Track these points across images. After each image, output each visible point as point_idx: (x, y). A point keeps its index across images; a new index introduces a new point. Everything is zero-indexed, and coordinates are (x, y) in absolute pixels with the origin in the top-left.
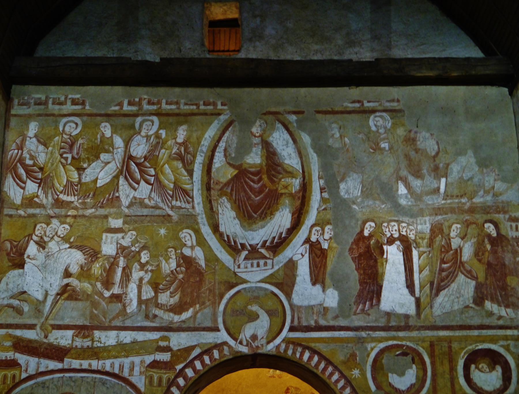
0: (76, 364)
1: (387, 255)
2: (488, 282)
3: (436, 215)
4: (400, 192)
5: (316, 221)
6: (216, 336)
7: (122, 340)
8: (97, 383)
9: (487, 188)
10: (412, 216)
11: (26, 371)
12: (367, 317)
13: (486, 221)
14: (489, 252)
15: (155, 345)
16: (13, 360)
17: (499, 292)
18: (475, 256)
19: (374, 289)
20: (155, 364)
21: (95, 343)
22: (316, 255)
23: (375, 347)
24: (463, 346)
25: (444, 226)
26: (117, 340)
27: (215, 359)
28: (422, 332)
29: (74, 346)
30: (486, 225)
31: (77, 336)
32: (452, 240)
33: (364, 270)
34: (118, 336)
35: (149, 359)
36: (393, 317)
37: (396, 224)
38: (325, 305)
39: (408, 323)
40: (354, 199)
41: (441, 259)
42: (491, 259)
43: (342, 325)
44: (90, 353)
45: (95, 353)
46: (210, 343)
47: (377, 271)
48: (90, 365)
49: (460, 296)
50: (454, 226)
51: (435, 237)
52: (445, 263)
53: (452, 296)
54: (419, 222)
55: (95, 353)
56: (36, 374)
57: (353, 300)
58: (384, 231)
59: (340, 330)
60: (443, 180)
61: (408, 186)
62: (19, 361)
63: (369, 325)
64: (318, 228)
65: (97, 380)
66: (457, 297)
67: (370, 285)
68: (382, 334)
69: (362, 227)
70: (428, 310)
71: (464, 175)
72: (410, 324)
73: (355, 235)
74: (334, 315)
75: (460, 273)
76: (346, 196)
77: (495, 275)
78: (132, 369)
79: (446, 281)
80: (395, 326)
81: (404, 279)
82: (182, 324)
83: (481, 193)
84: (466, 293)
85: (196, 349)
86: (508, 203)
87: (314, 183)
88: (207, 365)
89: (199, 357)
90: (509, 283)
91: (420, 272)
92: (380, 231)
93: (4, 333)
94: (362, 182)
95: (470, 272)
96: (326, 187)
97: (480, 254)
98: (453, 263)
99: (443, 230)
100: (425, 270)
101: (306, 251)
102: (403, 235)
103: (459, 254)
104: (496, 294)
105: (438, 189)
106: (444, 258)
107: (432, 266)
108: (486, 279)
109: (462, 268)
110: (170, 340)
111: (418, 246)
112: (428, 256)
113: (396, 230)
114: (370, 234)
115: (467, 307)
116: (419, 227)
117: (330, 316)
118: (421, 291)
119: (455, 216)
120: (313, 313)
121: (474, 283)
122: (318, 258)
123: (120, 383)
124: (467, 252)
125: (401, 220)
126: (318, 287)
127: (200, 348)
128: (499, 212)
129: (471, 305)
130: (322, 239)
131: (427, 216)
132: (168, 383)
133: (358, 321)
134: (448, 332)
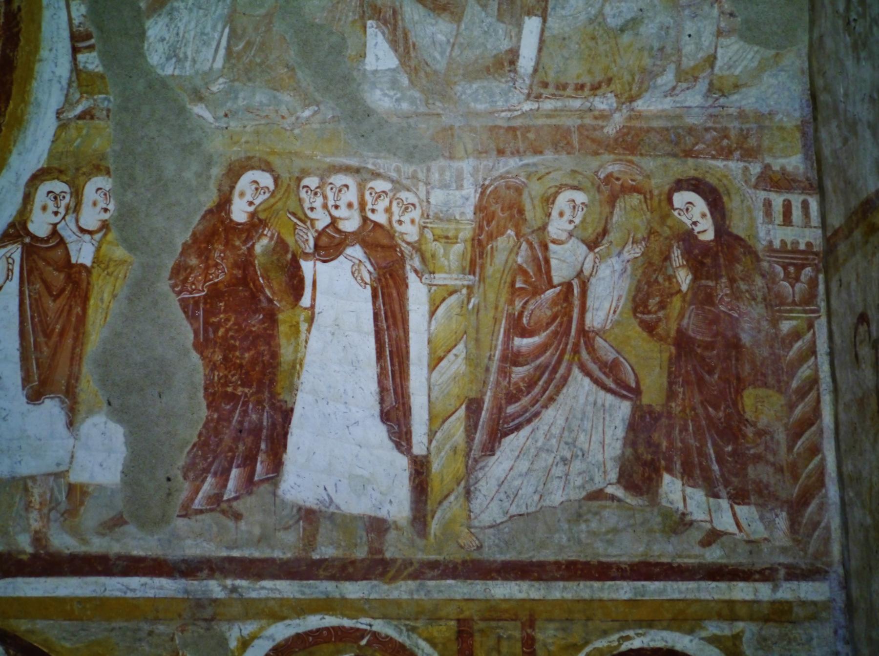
1: (314, 299)
2: (676, 407)
3: (501, 152)
4: (370, 63)
5: (51, 155)
9: (688, 63)
10: (410, 157)
12: (231, 524)
13: (680, 185)
17: (715, 444)
18: (635, 311)
19: (260, 420)
22: (48, 287)
23: (254, 637)
24: (576, 639)
28: (431, 583)
30: (680, 199)
32: (552, 246)
36: (325, 528)
37: (349, 180)
38: (77, 477)
39: (380, 551)
40: (198, 82)
41: (510, 316)
42: (691, 323)
43: (135, 553)
47: (274, 355)
49: (574, 456)
50: (563, 200)
51: (491, 237)
52: (525, 333)
57: (182, 460)
58: (306, 205)
59: (125, 573)
60: (532, 25)
61: (401, 42)
63: (236, 554)
64: (58, 186)
66: (564, 460)
67: (245, 404)
68: (286, 588)
69: (226, 188)
70: (453, 506)
71: (607, 9)
72: (388, 555)
73: (198, 218)
74: (107, 514)
75: (576, 371)
76: (169, 71)
77: (701, 382)
79: (525, 400)
80: (334, 560)
81: (374, 387)
83: (668, 78)
86: (760, 117)
87: (47, 14)
90: (749, 415)
92: (292, 204)
94: (230, 19)
95: (612, 368)
96: (92, 29)
97: (653, 302)
98: (555, 333)
99: (521, 212)
100: (451, 356)
101: (10, 271)
102: (377, 225)
103: (577, 302)
104: (702, 453)
105: (513, 56)
106: (521, 314)
107: (477, 340)
108: (671, 395)
111: (428, 266)
112: (463, 305)
113: (350, 205)
114: (253, 215)
115: (597, 495)
116: (438, 197)
117: (91, 516)
118: (431, 435)
119: (567, 162)
120: (28, 507)
121: (625, 408)
122: (56, 298)
124: (607, 296)
125: (370, 166)
126: (52, 409)
128: (727, 154)
129: (610, 490)
131: (467, 155)
133: (194, 541)
134: (525, 585)
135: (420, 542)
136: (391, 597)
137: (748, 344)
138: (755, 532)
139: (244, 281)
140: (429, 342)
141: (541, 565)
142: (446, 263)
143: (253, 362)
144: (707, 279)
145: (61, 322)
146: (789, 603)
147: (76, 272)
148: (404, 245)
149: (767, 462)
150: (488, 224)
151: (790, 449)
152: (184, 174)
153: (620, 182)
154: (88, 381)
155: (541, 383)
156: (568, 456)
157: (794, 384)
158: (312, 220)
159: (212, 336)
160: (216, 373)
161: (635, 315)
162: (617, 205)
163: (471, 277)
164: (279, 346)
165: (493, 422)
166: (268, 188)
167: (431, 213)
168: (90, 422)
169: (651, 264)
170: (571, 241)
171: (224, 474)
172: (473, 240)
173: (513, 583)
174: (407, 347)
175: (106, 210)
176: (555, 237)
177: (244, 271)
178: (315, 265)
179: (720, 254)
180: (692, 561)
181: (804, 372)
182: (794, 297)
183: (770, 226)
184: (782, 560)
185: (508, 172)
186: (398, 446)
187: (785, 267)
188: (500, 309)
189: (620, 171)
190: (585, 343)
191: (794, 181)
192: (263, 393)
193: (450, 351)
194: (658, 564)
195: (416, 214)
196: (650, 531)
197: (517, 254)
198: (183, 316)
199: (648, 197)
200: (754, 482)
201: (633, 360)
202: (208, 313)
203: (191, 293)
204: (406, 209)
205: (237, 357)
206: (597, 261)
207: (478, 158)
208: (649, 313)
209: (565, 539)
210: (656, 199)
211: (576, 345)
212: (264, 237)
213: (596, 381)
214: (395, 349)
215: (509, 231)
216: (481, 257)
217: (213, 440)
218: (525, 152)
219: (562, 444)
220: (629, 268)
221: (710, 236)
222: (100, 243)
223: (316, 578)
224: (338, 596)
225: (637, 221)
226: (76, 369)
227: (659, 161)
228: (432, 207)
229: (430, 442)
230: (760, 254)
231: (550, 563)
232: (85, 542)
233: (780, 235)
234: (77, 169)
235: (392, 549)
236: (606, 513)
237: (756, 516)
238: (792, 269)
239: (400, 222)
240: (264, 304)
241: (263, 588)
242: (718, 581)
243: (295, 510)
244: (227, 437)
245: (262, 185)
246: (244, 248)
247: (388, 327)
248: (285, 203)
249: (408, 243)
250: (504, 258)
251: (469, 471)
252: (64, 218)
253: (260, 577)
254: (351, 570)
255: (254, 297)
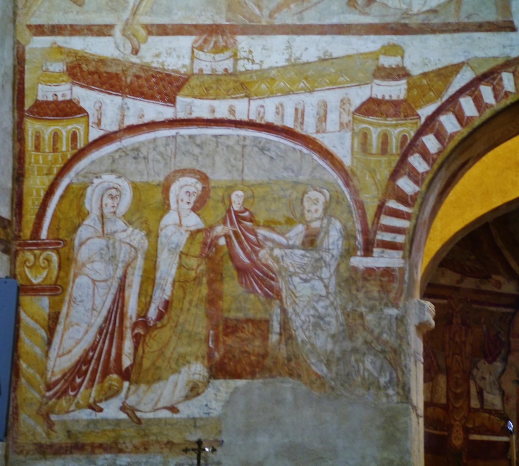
0: (201, 108)
6: (508, 43)
7: (298, 54)
8: (247, 150)
11: (99, 123)
15: (371, 66)
16: (70, 101)
20: (372, 107)
21: (241, 62)
26: (287, 56)
27: (507, 94)
29: (196, 71)
31: (201, 48)
34: (289, 47)
35: (359, 96)
44: (231, 85)
45: (240, 84)
46: (495, 58)
48: (232, 111)
55: (240, 84)
56: (120, 131)
62: (82, 104)
65: (247, 142)
78: (322, 118)
82: (431, 16)
85: (462, 72)
88: (487, 106)
89: (471, 88)
93: (49, 45)
110: (404, 52)
123: (299, 147)
127: (472, 69)
132: (401, 147)
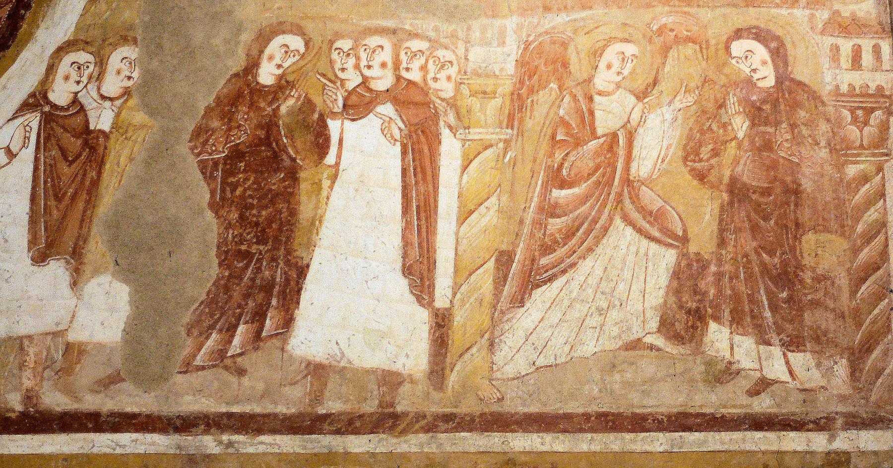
1: (339, 156)
2: (728, 253)
3: (547, 9)
5: (78, 28)
12: (233, 379)
13: (738, 34)
14: (739, 146)
17: (768, 292)
18: (685, 159)
19: (273, 278)
22: (64, 152)
25: (571, 50)
28: (443, 436)
30: (738, 47)
32: (597, 98)
33: (244, 207)
36: (333, 383)
39: (392, 405)
42: (748, 171)
43: (128, 409)
47: (293, 213)
50: (611, 54)
51: (531, 91)
52: (563, 184)
53: (578, 306)
54: (476, 34)
57: (187, 317)
58: (338, 66)
59: (116, 428)
63: (236, 409)
64: (83, 57)
66: (600, 310)
69: (255, 53)
70: (477, 356)
72: (399, 409)
74: (102, 372)
75: (618, 221)
79: (561, 252)
80: (340, 414)
81: (398, 241)
84: (635, 294)
90: (807, 261)
91: (464, 215)
92: (322, 66)
95: (656, 217)
97: (705, 152)
98: (598, 183)
99: (565, 65)
100: (482, 209)
101: (27, 138)
102: (410, 82)
103: (621, 152)
104: (752, 300)
106: (561, 166)
107: (512, 193)
108: (722, 243)
109: (627, 203)
111: (463, 121)
113: (384, 65)
114: (280, 77)
115: (635, 345)
116: (477, 55)
117: (87, 373)
119: (617, 15)
121: (668, 257)
122: (71, 163)
125: (407, 27)
126: (57, 270)
129: (649, 339)
130: (94, 94)
131: (511, 12)
134: (548, 437)
135: (436, 395)
136: (399, 450)
137: (809, 190)
138: (810, 380)
139: (267, 141)
140: (460, 196)
141: (568, 417)
142: (483, 118)
143: (270, 221)
144: (766, 125)
145: (73, 185)
146: (847, 454)
147: (93, 138)
148: (438, 101)
149: (826, 308)
150: (530, 78)
151: (853, 293)
152: (212, 41)
153: (674, 33)
154: (97, 242)
155: (579, 234)
156: (605, 306)
157: (860, 228)
158: (342, 80)
159: (229, 195)
160: (231, 232)
161: (685, 163)
162: (670, 54)
163: (509, 131)
164: (299, 203)
165: (524, 271)
166: (298, 51)
167: (469, 70)
168: (94, 282)
169: (704, 112)
170: (618, 92)
171: (232, 329)
172: (512, 94)
173: (535, 436)
174: (436, 201)
175: (129, 78)
176: (601, 88)
177: (268, 132)
178: (342, 124)
179: (781, 100)
180: (739, 411)
181: (872, 215)
182: (862, 141)
183: (837, 71)
184: (841, 408)
185: (554, 28)
186: (419, 299)
187: (852, 111)
188: (538, 161)
189: (675, 23)
190: (629, 193)
191: (865, 26)
192: (279, 249)
193: (481, 204)
194: (698, 415)
195: (453, 71)
196: (692, 381)
197: (559, 107)
198: (201, 177)
199: (704, 46)
200: (811, 328)
201: (681, 208)
202: (227, 173)
203: (210, 154)
204: (443, 67)
205: (254, 216)
206: (646, 111)
207: (522, 15)
208: (701, 160)
209: (596, 390)
210: (712, 49)
211: (620, 195)
212: (290, 98)
213: (640, 231)
214: (422, 204)
215: (552, 85)
216: (520, 110)
217: (223, 297)
218: (573, 8)
219: (598, 295)
220: (680, 117)
221: (771, 82)
222: (120, 109)
223: (320, 432)
224: (342, 451)
225: (691, 70)
226: (85, 230)
227: (718, 11)
228: (471, 64)
229: (454, 295)
230: (825, 99)
231: (577, 415)
232: (78, 399)
233: (848, 79)
234: (104, 41)
235: (404, 402)
236: (643, 363)
237: (813, 363)
238: (860, 113)
239: (435, 79)
240: (287, 163)
241: (262, 443)
242: (766, 430)
243: (303, 365)
244: (237, 294)
245: (292, 48)
246: (269, 109)
247: (417, 183)
248: (315, 65)
249: (443, 100)
250: (545, 111)
251: (494, 323)
252: (86, 86)
253: (259, 431)
254: (358, 424)
255: (276, 156)
